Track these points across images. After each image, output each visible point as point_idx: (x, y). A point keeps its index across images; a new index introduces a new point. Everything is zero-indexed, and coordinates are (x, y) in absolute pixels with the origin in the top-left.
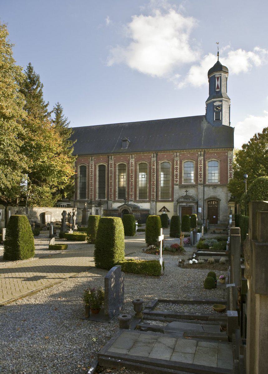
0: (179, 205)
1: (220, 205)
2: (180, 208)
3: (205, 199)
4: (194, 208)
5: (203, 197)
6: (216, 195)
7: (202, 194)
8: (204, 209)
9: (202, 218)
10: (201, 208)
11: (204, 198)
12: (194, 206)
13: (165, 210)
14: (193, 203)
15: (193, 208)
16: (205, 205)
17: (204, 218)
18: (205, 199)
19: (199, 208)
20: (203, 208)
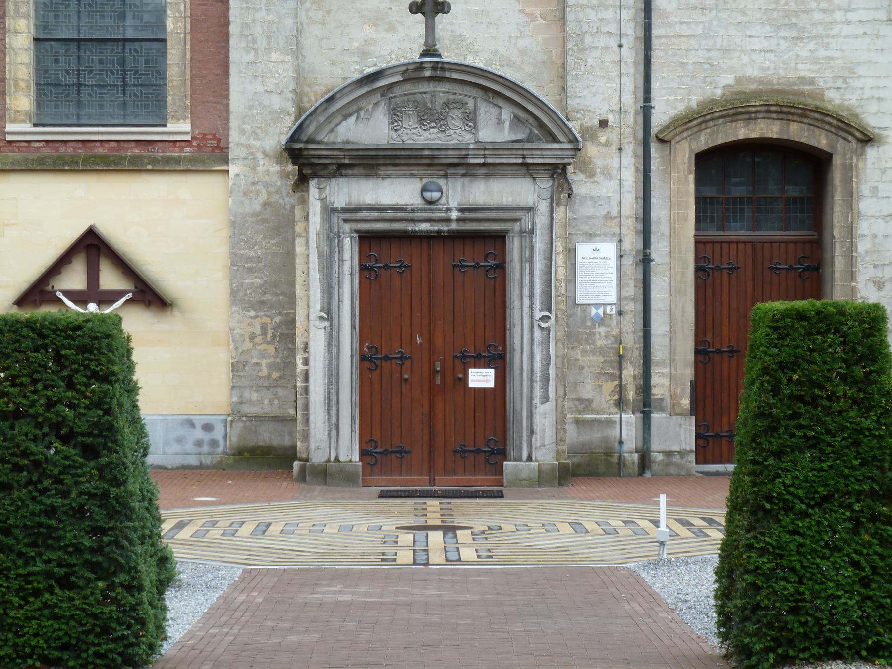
0: (329, 211)
1: (866, 206)
2: (332, 238)
3: (661, 117)
4: (539, 244)
5: (631, 100)
6: (805, 70)
7: (630, 54)
8: (645, 261)
9: (621, 388)
10: (609, 250)
11: (646, 109)
12: (541, 220)
13: (110, 280)
14: (528, 169)
15: (514, 246)
16: (659, 212)
17: (645, 388)
18: (661, 117)
19: (584, 250)
20: (632, 242)
